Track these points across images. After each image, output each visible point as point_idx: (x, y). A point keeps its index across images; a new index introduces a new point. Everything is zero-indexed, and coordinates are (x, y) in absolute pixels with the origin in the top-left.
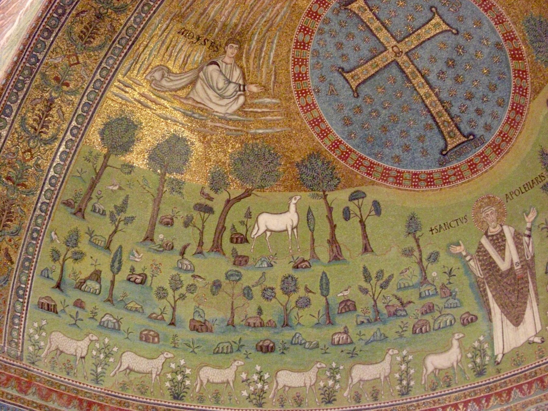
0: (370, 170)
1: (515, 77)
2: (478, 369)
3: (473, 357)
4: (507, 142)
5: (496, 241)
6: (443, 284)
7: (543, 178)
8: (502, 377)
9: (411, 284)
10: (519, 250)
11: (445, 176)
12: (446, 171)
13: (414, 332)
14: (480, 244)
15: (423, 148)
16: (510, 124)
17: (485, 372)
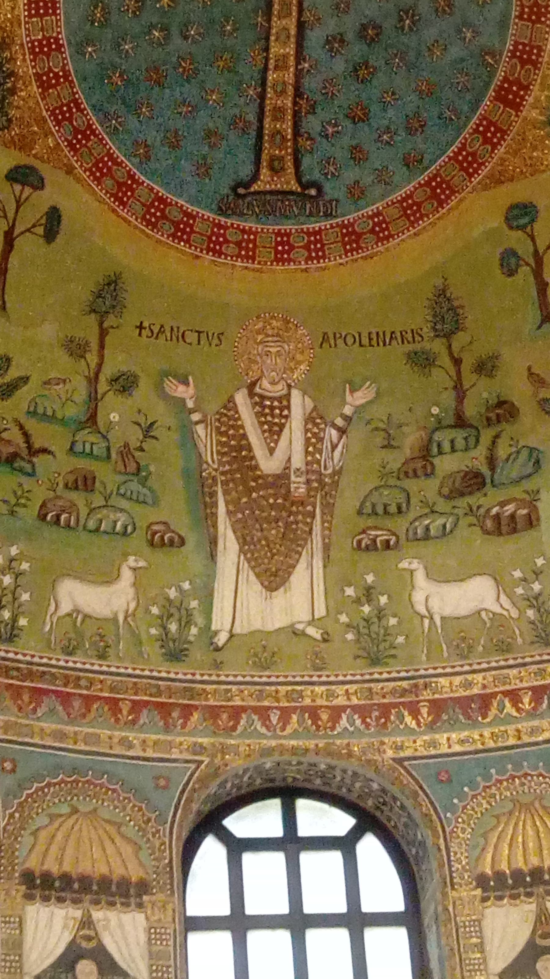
0: (79, 141)
1: (476, 131)
2: (171, 644)
3: (161, 617)
4: (378, 237)
5: (267, 411)
6: (126, 445)
7: (417, 338)
8: (223, 678)
9: (59, 415)
10: (311, 449)
11: (218, 236)
12: (226, 228)
13: (42, 517)
14: (231, 400)
15: (204, 158)
16: (405, 210)
17: (186, 655)
